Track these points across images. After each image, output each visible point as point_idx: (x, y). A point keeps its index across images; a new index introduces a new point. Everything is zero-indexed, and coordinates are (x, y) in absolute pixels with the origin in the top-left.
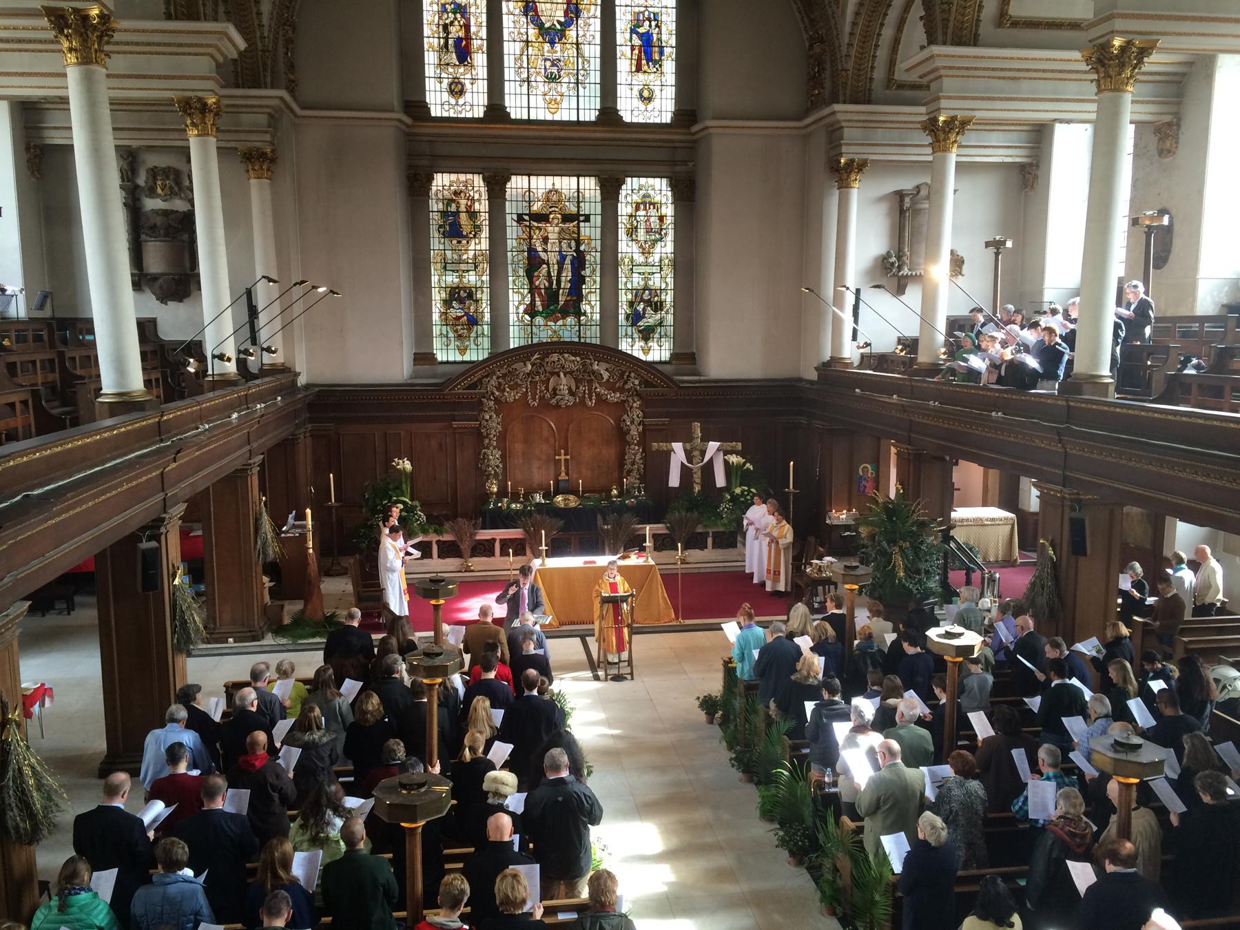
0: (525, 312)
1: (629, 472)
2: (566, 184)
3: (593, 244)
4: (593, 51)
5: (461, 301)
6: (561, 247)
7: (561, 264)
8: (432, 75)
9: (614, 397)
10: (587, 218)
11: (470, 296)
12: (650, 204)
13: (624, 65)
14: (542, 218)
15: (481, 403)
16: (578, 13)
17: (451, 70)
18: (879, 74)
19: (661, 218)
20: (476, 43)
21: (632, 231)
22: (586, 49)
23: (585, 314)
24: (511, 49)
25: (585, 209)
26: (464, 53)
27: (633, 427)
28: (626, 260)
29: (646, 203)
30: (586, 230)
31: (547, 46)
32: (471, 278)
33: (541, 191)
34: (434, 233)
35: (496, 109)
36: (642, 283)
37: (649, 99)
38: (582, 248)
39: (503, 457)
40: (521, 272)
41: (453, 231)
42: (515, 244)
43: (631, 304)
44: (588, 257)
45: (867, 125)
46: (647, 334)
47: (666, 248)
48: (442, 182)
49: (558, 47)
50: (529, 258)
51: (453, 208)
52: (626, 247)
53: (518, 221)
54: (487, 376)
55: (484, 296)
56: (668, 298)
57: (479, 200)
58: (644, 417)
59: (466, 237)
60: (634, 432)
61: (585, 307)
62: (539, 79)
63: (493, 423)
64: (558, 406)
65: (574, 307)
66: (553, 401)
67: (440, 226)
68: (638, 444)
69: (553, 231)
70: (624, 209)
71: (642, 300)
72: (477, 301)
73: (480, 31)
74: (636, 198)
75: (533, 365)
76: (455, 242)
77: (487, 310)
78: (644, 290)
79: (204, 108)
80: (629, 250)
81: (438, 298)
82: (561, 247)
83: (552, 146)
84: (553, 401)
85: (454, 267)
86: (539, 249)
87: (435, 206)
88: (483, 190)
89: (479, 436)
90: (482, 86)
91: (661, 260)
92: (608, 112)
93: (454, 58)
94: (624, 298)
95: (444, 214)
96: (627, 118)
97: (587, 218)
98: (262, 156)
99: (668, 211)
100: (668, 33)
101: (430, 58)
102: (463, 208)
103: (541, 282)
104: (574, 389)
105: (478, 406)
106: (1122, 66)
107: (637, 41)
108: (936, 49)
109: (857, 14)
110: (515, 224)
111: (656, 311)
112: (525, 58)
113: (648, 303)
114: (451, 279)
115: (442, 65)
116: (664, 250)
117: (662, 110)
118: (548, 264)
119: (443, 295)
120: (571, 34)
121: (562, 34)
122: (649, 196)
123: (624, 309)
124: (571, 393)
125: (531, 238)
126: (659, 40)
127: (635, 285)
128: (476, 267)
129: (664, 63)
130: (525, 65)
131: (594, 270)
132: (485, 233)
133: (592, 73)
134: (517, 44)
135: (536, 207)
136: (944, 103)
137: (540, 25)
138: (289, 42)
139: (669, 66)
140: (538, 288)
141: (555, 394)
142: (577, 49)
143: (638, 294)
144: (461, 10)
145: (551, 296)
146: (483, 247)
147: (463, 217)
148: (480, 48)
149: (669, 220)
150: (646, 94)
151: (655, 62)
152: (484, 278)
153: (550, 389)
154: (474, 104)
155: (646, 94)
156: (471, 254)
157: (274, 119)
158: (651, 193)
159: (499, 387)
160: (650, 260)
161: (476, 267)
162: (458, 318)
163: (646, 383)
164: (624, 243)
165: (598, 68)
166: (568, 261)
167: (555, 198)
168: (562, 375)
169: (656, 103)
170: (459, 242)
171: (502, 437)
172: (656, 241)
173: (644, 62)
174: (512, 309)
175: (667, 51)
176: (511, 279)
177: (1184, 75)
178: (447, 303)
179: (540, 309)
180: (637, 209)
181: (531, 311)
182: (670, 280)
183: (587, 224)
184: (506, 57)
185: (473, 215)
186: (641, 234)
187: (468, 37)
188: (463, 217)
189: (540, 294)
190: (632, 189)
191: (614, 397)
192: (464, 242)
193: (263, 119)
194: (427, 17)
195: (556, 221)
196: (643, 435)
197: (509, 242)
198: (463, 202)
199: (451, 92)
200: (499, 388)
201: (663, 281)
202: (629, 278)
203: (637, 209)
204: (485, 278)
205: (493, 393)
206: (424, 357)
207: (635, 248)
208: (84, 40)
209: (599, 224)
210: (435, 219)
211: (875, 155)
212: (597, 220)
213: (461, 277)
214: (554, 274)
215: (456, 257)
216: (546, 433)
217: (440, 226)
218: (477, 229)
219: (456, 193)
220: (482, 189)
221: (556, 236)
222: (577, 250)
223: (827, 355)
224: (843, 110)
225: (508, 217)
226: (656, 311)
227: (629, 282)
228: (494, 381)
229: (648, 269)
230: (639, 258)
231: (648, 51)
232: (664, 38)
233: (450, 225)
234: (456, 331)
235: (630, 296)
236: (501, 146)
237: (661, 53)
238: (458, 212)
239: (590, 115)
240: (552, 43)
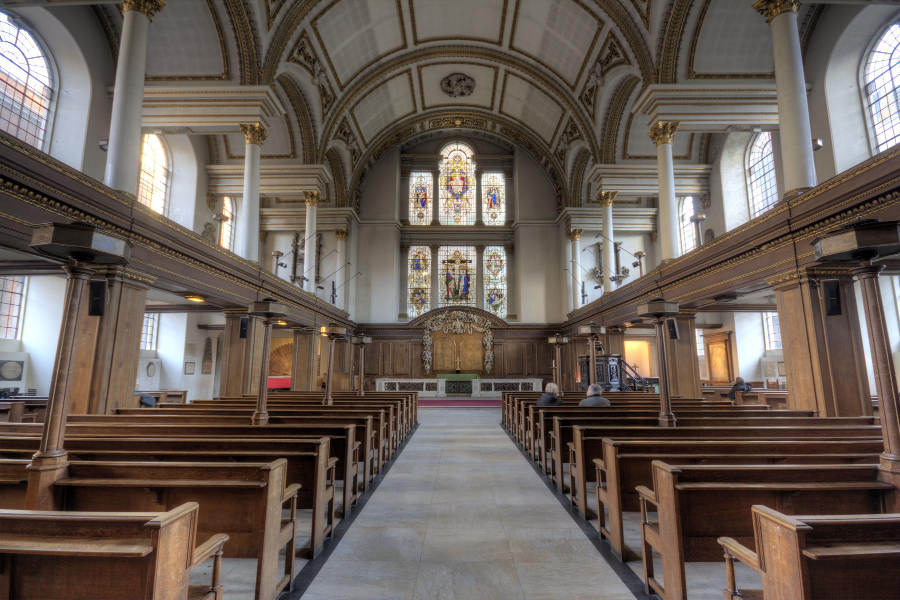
2: (463, 250)
4: (473, 202)
5: (419, 294)
7: (460, 280)
9: (481, 330)
10: (471, 262)
13: (485, 206)
16: (467, 189)
18: (584, 198)
19: (501, 261)
20: (429, 200)
22: (470, 201)
24: (442, 202)
25: (470, 258)
26: (424, 204)
29: (495, 256)
30: (470, 266)
32: (424, 286)
34: (409, 267)
35: (435, 222)
37: (495, 217)
39: (432, 355)
41: (417, 267)
45: (581, 216)
46: (496, 307)
47: (504, 273)
55: (428, 292)
56: (505, 293)
60: (488, 344)
61: (469, 296)
63: (428, 339)
65: (465, 296)
70: (485, 258)
73: (430, 196)
79: (312, 196)
83: (457, 235)
87: (410, 258)
88: (430, 252)
89: (422, 345)
90: (430, 214)
92: (479, 222)
94: (486, 293)
95: (414, 260)
96: (486, 224)
97: (471, 262)
98: (342, 232)
99: (504, 258)
100: (502, 194)
101: (411, 206)
103: (452, 286)
105: (423, 333)
106: (664, 133)
108: (597, 166)
109: (572, 174)
113: (496, 295)
114: (415, 286)
115: (415, 207)
117: (500, 219)
120: (465, 195)
121: (461, 195)
123: (486, 297)
124: (462, 328)
132: (429, 268)
136: (603, 187)
137: (453, 194)
138: (357, 197)
139: (503, 206)
143: (492, 291)
144: (424, 189)
145: (456, 292)
147: (421, 262)
149: (505, 262)
154: (427, 220)
157: (349, 220)
159: (432, 325)
169: (498, 219)
171: (432, 346)
177: (709, 174)
178: (414, 295)
181: (448, 298)
182: (505, 286)
185: (425, 260)
186: (493, 268)
187: (426, 198)
188: (421, 262)
190: (490, 250)
191: (481, 330)
193: (344, 220)
194: (411, 191)
196: (493, 345)
201: (503, 287)
202: (488, 285)
204: (429, 285)
206: (403, 315)
208: (253, 135)
210: (410, 262)
211: (585, 228)
212: (474, 263)
218: (426, 266)
223: (571, 309)
224: (569, 210)
227: (488, 287)
228: (429, 322)
230: (492, 277)
231: (494, 201)
236: (438, 235)
239: (472, 223)
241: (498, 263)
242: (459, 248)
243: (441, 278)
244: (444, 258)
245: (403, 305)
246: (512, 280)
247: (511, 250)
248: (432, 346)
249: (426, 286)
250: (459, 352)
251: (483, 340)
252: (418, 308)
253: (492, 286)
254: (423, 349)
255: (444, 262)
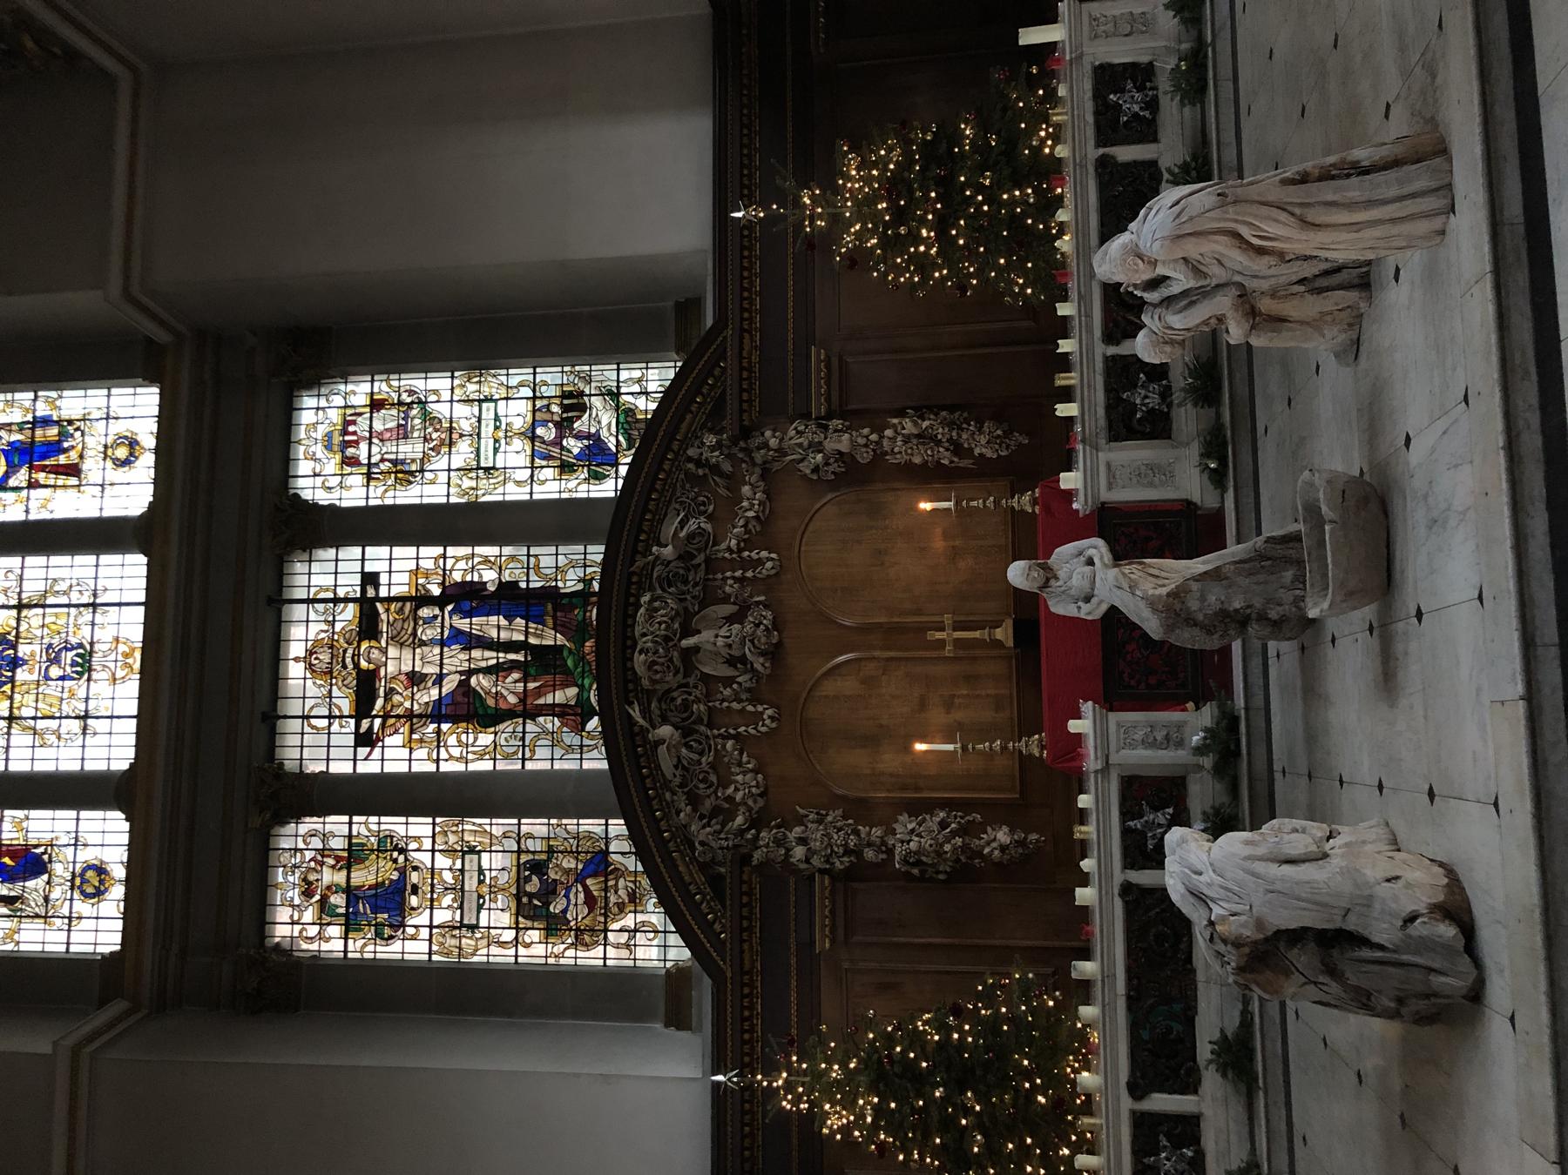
0: (580, 728)
1: (957, 449)
3: (427, 564)
5: (549, 891)
6: (432, 642)
7: (470, 642)
8: (63, 936)
10: (370, 579)
11: (538, 868)
12: (345, 432)
14: (366, 687)
15: (766, 864)
17: (56, 894)
21: (403, 473)
22: (32, 588)
23: (587, 581)
25: (350, 584)
27: (830, 445)
28: (467, 483)
29: (343, 443)
30: (397, 584)
31: (21, 675)
33: (312, 690)
34: (391, 951)
36: (517, 444)
37: (133, 444)
38: (436, 591)
39: (918, 808)
40: (486, 739)
41: (388, 904)
42: (421, 753)
43: (565, 468)
44: (457, 577)
47: (439, 388)
48: (295, 924)
49: (23, 650)
50: (455, 719)
51: (338, 900)
52: (430, 492)
53: (372, 745)
54: (693, 849)
56: (552, 378)
57: (325, 837)
58: (806, 416)
59: (403, 872)
60: (843, 443)
61: (570, 583)
62: (82, 693)
64: (774, 653)
66: (759, 663)
67: (379, 935)
68: (880, 430)
69: (397, 661)
70: (354, 494)
71: (557, 442)
72: (551, 851)
74: (331, 465)
75: (665, 720)
76: (414, 901)
77: (570, 822)
78: (533, 438)
80: (443, 477)
81: (540, 950)
82: (432, 642)
84: (759, 663)
85: (470, 904)
86: (435, 693)
87: (333, 943)
88: (309, 824)
89: (855, 875)
91: (468, 401)
93: (38, 883)
94: (551, 487)
97: (370, 579)
99: (359, 391)
102: (340, 878)
103: (510, 689)
104: (728, 609)
105: (778, 874)
107: (20, 478)
110: (377, 752)
111: (582, 408)
112: (41, 724)
113: (564, 426)
114: (498, 917)
116: (446, 395)
117: (137, 408)
118: (470, 673)
119: (534, 935)
122: (329, 435)
125: (410, 715)
126: (21, 427)
127: (523, 460)
128: (472, 850)
129: (65, 414)
130: (53, 724)
131: (486, 560)
132: (395, 825)
133: (78, 573)
134: (14, 740)
135: (346, 705)
139: (73, 402)
140: (524, 697)
141: (743, 659)
142: (30, 606)
143: (541, 453)
145: (542, 662)
146: (428, 830)
147: (363, 877)
148: (18, 825)
149: (382, 388)
150: (122, 453)
151: (63, 435)
152: (497, 831)
153: (730, 672)
155: (122, 453)
156: (442, 862)
158: (322, 430)
160: (466, 426)
161: (472, 850)
162: (590, 901)
163: (714, 420)
164: (428, 489)
165: (65, 560)
166: (462, 624)
167: (325, 657)
168: (685, 643)
170: (415, 890)
172: (428, 418)
173: (62, 459)
174: (570, 765)
175: (42, 410)
176: (501, 766)
178: (554, 927)
179: (572, 692)
180: (352, 462)
181: (574, 715)
182: (518, 375)
183: (384, 579)
184: (40, 767)
185: (353, 855)
186: (411, 450)
189: (539, 692)
190: (318, 479)
191: (751, 496)
192: (414, 877)
195: (375, 654)
196: (854, 417)
197: (417, 767)
198: (328, 877)
199: (99, 893)
200: (723, 813)
203: (352, 462)
204: (499, 826)
205: (741, 832)
207: (442, 463)
209: (383, 551)
210: (363, 947)
213: (494, 890)
214: (490, 658)
215: (447, 900)
216: (847, 685)
217: (379, 935)
218: (390, 846)
219: (308, 893)
220: (303, 829)
221: (407, 654)
222: (440, 602)
225: (363, 768)
226: (582, 408)
227: (521, 479)
228: (700, 832)
229: (487, 430)
230: (462, 453)
232: (16, 416)
233: (375, 910)
234: (621, 908)
235: (549, 473)
237: (46, 422)
238: (350, 891)
240: (15, 663)
241: (385, 421)
242: (296, 649)
243: (465, 753)
244: (344, 733)
245: (616, 998)
246: (476, 333)
247: (321, 351)
248: (860, 810)
249: (497, 845)
250: (892, 633)
251: (818, 483)
252: (635, 899)
253: (515, 455)
254: (881, 871)
255: (365, 739)
